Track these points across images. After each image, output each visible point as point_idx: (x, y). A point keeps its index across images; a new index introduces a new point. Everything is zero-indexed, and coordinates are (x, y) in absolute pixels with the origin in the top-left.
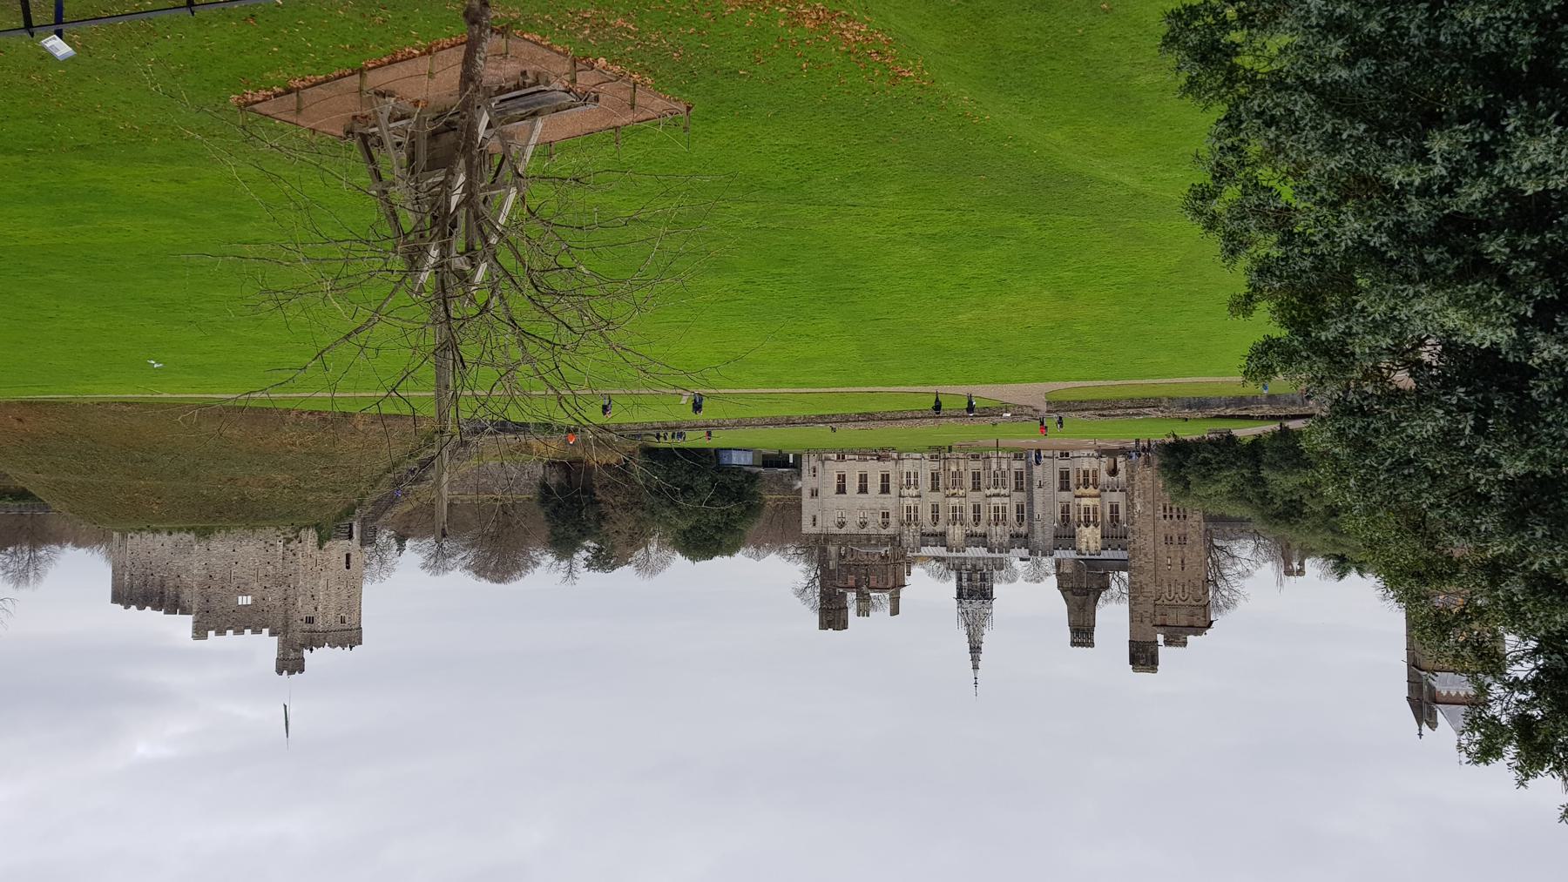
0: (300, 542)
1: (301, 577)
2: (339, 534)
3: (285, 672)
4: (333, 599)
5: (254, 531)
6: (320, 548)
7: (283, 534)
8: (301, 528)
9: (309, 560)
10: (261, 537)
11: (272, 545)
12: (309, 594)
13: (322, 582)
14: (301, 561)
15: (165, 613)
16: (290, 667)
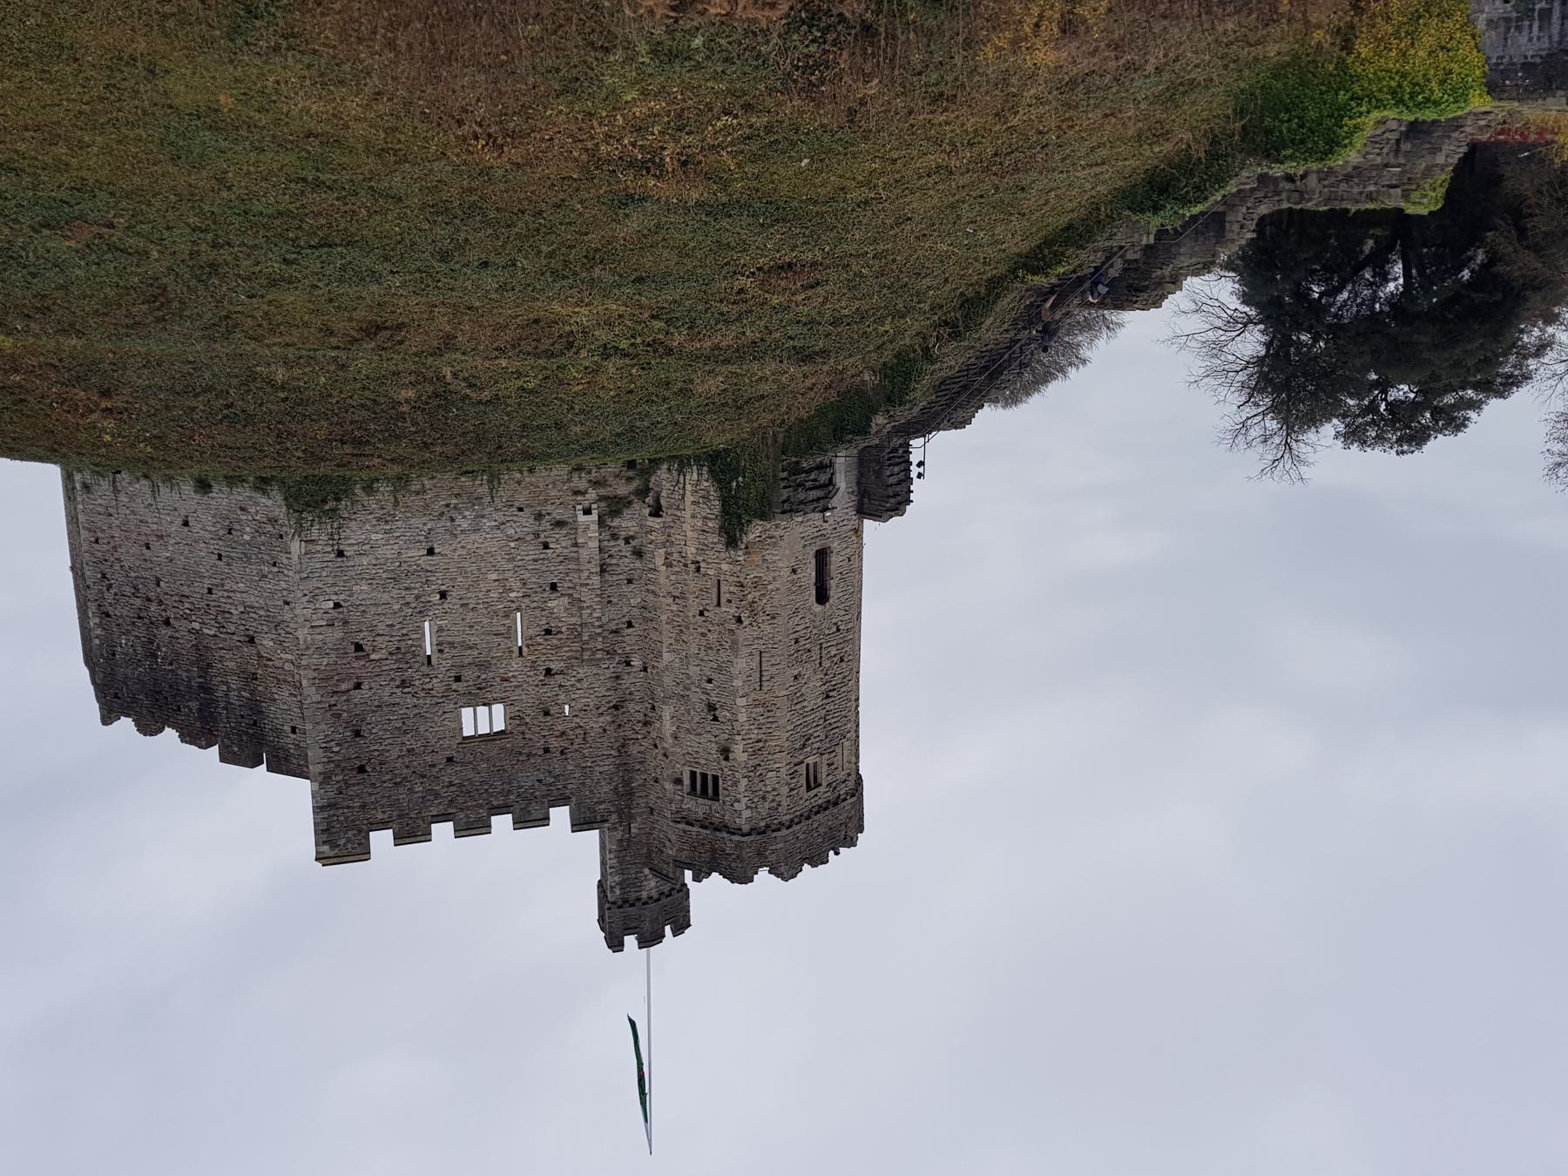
0: (657, 512)
1: (667, 635)
2: (801, 495)
3: (630, 941)
4: (783, 715)
5: (494, 479)
6: (732, 542)
7: (596, 484)
8: (655, 463)
9: (693, 583)
10: (521, 499)
11: (560, 524)
12: (696, 697)
13: (741, 664)
14: (664, 578)
15: (223, 759)
16: (647, 926)
